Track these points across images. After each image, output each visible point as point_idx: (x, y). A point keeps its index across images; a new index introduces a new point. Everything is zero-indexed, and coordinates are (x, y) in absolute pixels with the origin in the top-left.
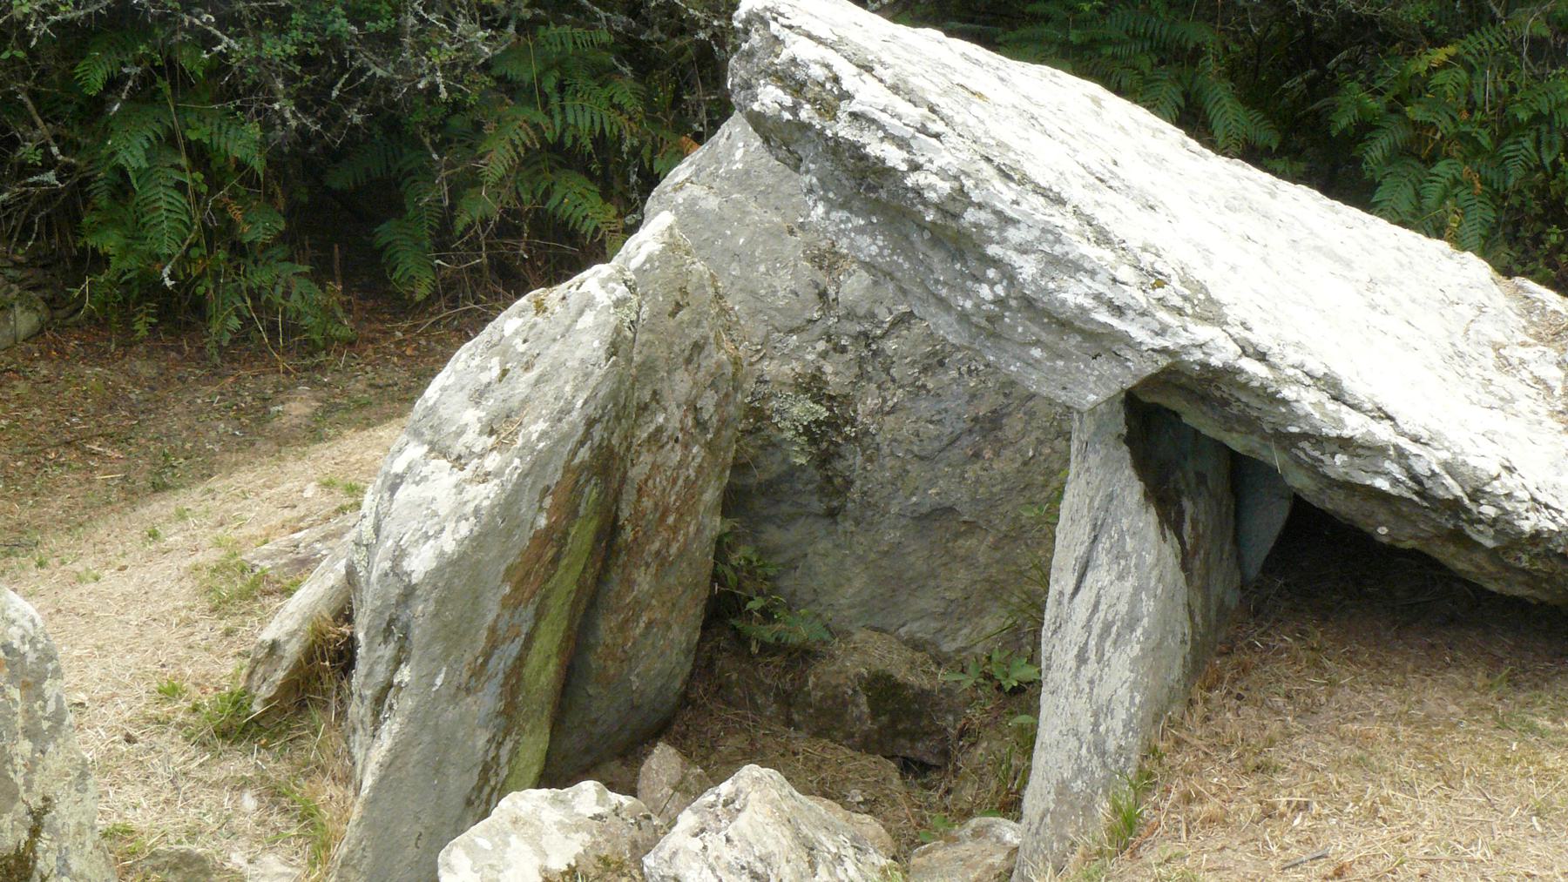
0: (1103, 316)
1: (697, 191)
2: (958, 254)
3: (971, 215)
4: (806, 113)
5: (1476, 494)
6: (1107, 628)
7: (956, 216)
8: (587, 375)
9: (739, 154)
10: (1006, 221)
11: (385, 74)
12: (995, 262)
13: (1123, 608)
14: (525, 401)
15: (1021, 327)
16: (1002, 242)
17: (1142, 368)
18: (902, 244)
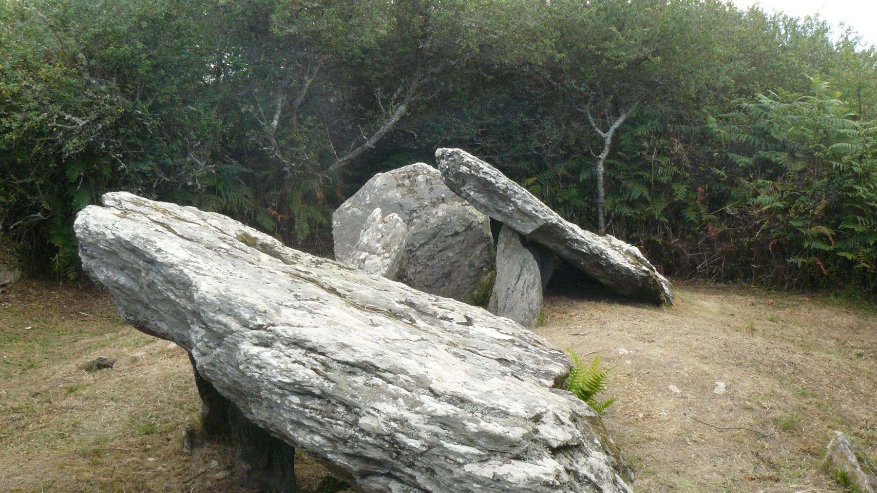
0: (534, 212)
1: (355, 210)
2: (504, 201)
3: (509, 192)
4: (473, 172)
5: (602, 253)
6: (528, 286)
7: (506, 192)
8: (404, 236)
9: (368, 199)
10: (516, 193)
11: (169, 180)
12: (513, 202)
13: (532, 281)
14: (390, 242)
15: (517, 216)
16: (515, 198)
17: (541, 223)
18: (491, 199)
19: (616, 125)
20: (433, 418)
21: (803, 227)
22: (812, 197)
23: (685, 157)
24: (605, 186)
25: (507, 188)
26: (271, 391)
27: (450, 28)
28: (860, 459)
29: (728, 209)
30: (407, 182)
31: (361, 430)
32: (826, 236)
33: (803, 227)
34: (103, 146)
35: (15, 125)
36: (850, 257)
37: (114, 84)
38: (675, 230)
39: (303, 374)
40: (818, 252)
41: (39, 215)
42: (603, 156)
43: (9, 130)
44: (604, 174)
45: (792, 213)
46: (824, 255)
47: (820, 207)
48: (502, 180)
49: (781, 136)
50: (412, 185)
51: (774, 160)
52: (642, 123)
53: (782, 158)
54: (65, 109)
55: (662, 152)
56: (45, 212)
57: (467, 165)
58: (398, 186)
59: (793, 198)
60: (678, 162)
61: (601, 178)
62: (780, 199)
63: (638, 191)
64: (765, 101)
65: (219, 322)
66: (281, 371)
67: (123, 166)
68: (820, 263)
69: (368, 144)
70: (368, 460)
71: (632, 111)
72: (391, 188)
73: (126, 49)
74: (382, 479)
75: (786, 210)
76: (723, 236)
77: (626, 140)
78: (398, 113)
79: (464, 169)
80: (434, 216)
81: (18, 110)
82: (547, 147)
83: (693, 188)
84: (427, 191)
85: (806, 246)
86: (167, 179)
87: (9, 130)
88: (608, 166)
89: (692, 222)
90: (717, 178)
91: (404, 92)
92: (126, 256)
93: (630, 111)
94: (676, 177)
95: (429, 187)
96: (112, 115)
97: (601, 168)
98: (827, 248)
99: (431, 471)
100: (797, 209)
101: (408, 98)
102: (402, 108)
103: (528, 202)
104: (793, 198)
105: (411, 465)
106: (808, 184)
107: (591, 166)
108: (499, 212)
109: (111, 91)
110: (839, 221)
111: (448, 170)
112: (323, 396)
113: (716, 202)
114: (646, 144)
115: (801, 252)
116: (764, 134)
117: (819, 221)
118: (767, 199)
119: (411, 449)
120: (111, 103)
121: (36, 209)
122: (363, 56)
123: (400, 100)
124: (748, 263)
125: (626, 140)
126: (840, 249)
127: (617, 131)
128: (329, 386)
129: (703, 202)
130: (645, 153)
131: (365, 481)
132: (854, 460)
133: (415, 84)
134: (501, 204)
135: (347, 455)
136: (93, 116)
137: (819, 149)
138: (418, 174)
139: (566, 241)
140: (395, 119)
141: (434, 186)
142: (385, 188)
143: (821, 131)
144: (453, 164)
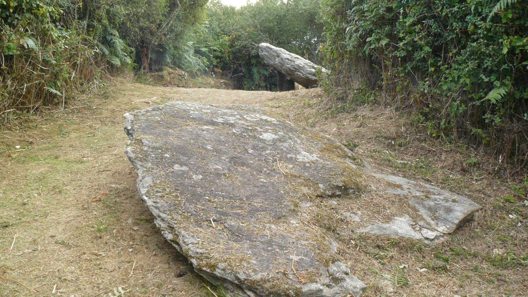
20: (304, 63)
35: (239, 44)
37: (267, 35)
39: (288, 57)
43: (237, 45)
54: (253, 41)
56: (243, 73)
70: (296, 68)
73: (272, 24)
81: (240, 40)
87: (237, 45)
99: (303, 70)
109: (266, 37)
112: (291, 60)
121: (241, 72)
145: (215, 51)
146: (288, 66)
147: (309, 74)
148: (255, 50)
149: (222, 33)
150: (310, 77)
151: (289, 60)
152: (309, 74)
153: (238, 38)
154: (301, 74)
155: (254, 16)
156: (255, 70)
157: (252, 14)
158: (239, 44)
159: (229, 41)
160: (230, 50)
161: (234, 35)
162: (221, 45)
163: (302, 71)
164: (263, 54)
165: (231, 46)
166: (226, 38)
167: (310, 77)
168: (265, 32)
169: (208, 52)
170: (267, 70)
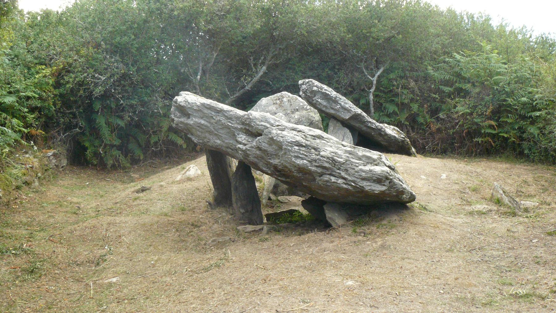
2: (335, 103)
3: (337, 99)
5: (382, 128)
10: (341, 99)
12: (339, 103)
15: (341, 110)
18: (329, 102)
19: (379, 73)
20: (346, 152)
21: (481, 122)
22: (485, 106)
23: (416, 89)
24: (374, 106)
25: (336, 97)
26: (287, 145)
27: (290, 24)
28: (504, 192)
29: (441, 115)
30: (278, 102)
31: (322, 156)
32: (493, 126)
33: (481, 122)
34: (113, 91)
35: (71, 80)
36: (506, 136)
37: (118, 58)
38: (413, 128)
39: (299, 138)
40: (489, 134)
41: (77, 129)
42: (372, 90)
43: (68, 82)
44: (373, 100)
45: (475, 115)
46: (493, 136)
47: (489, 111)
48: (334, 94)
49: (467, 75)
50: (281, 103)
51: (464, 88)
52: (392, 72)
53: (468, 86)
54: (95, 71)
55: (404, 87)
56: (81, 128)
57: (316, 86)
58: (274, 104)
59: (475, 107)
60: (413, 92)
61: (372, 102)
62: (468, 108)
63: (391, 108)
64: (458, 57)
65: (261, 125)
66: (291, 138)
67: (122, 102)
68: (490, 140)
69: (247, 88)
70: (324, 168)
71: (387, 65)
72: (270, 105)
73: (125, 39)
74: (328, 176)
75: (471, 114)
76: (439, 130)
77: (385, 81)
78: (262, 71)
79: (315, 88)
80: (293, 119)
81: (73, 72)
82: (341, 87)
83: (421, 106)
84: (289, 106)
85: (483, 131)
86: (142, 109)
87: (68, 82)
88: (376, 96)
89: (422, 124)
90: (434, 99)
91: (265, 59)
92: (206, 111)
93: (386, 66)
94: (412, 100)
95: (290, 103)
96: (118, 74)
97: (371, 97)
98: (494, 132)
99: (346, 170)
100: (477, 112)
101: (267, 62)
102: (264, 68)
103: (346, 103)
104: (475, 107)
105: (339, 169)
106: (483, 99)
107: (366, 96)
108: (332, 108)
109: (117, 61)
110: (499, 118)
111: (307, 90)
112: (306, 146)
113: (434, 112)
114: (395, 83)
115: (480, 135)
116: (458, 75)
117: (490, 118)
118: (461, 109)
119: (339, 162)
120: (117, 68)
121: (76, 126)
122: (244, 40)
123: (263, 63)
124: (453, 143)
125: (385, 81)
126: (500, 132)
127: (379, 77)
128: (308, 143)
129: (427, 113)
130: (395, 88)
131: (322, 177)
132: (502, 192)
133: (271, 55)
134: (334, 104)
135: (316, 166)
136: (108, 75)
137: (487, 80)
138: (283, 98)
139: (365, 122)
140: (261, 74)
141: (292, 103)
142: (267, 105)
143: (488, 71)
144: (309, 87)
145: (28, 98)
146: (299, 162)
147: (364, 179)
148: (100, 88)
149: (36, 61)
150: (369, 186)
151: (299, 145)
152: (364, 179)
153: (68, 69)
154: (340, 181)
155: (92, 27)
156: (101, 121)
157: (90, 23)
158: (71, 80)
159: (53, 75)
160: (57, 92)
161: (60, 62)
162: (38, 85)
163: (343, 174)
164: (190, 122)
165: (57, 85)
166: (48, 71)
167: (367, 188)
168: (113, 53)
169: (17, 104)
170: (122, 118)
